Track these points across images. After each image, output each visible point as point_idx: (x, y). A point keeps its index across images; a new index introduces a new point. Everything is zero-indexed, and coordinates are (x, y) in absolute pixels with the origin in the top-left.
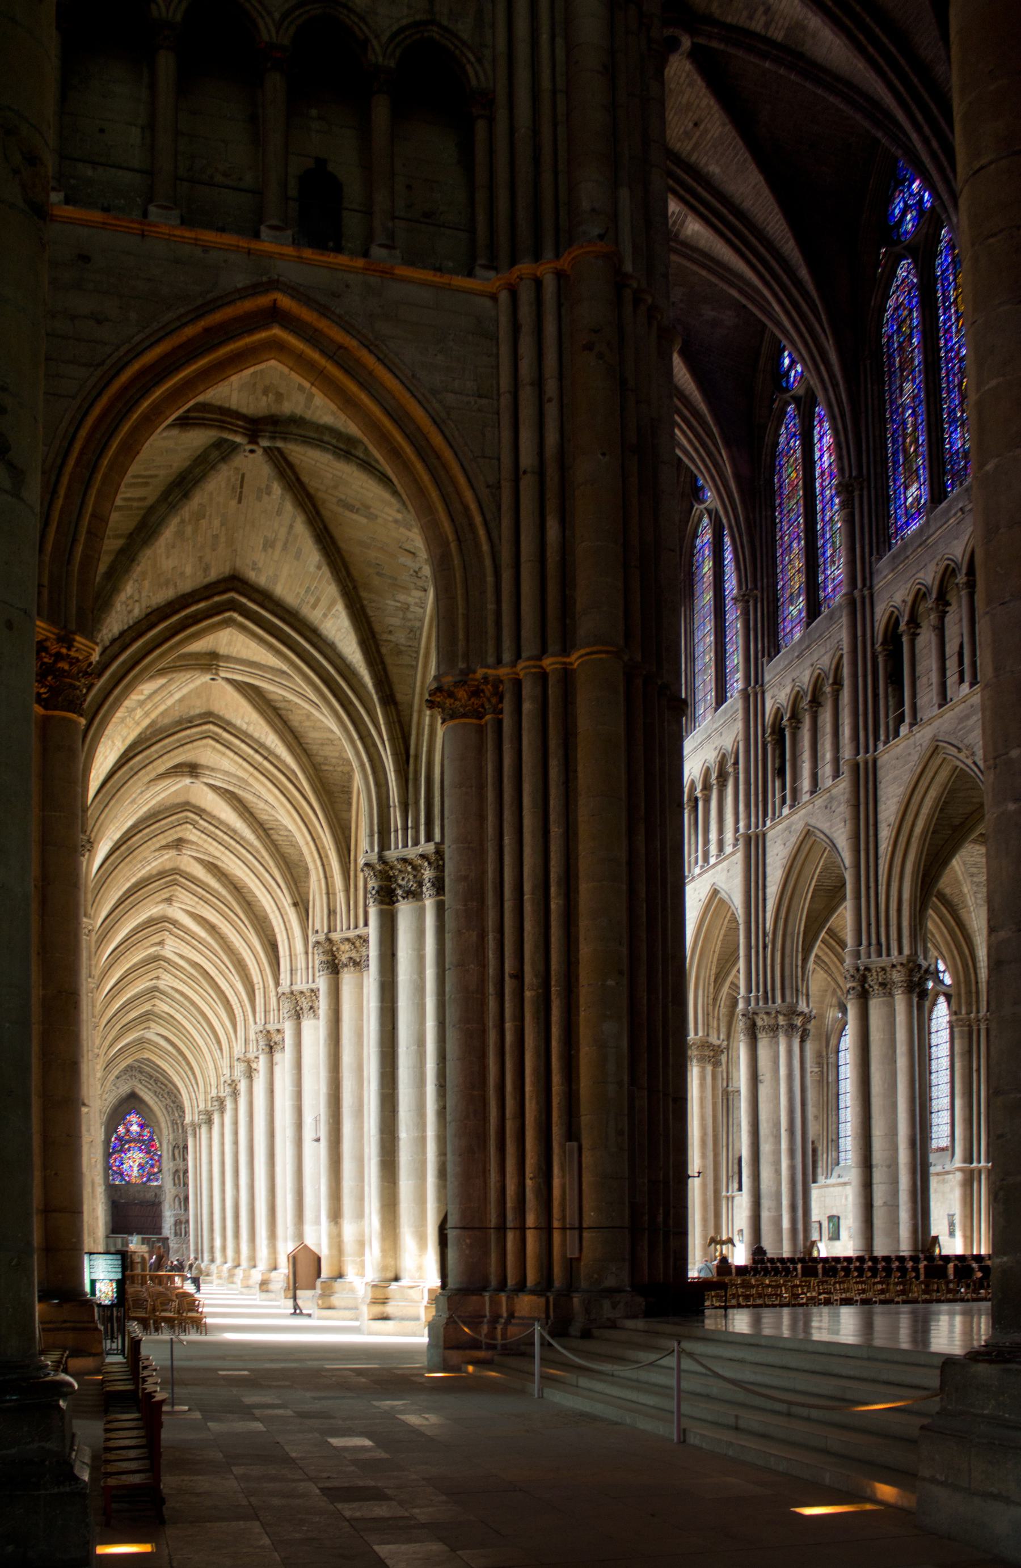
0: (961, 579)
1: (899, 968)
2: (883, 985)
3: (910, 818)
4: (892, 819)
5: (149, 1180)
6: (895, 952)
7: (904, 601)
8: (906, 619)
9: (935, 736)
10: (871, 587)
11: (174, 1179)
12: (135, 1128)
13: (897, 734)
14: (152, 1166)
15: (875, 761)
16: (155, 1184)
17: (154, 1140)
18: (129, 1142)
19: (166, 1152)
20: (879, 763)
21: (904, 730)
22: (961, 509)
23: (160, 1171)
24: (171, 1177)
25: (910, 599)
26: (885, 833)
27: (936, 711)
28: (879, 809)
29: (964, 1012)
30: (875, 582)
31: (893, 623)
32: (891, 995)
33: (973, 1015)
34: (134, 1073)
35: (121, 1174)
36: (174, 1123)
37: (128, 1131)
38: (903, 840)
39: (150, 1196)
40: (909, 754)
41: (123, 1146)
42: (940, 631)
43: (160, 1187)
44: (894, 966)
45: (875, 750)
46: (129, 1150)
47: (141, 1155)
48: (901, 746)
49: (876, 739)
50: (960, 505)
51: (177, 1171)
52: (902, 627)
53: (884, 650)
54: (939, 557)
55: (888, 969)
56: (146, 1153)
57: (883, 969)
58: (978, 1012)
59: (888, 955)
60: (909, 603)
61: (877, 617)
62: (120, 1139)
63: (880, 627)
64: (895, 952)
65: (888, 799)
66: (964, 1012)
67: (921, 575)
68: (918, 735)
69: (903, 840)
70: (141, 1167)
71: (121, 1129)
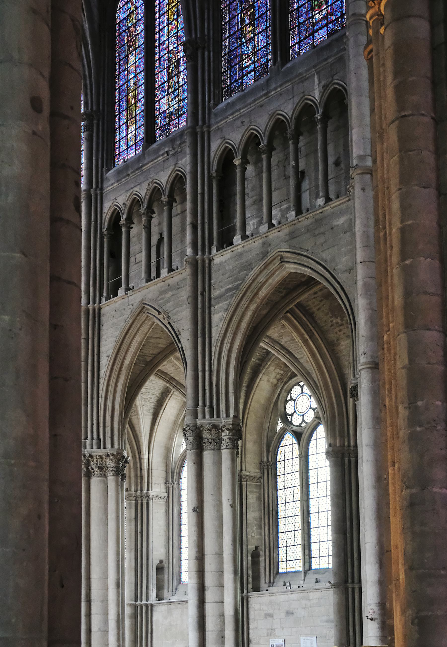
0: (165, 198)
1: (111, 457)
2: (101, 468)
3: (122, 353)
4: (110, 352)
6: (109, 445)
7: (124, 204)
8: (125, 216)
9: (143, 300)
10: (102, 189)
13: (116, 295)
15: (100, 309)
20: (103, 311)
21: (121, 291)
22: (167, 152)
25: (128, 204)
26: (105, 362)
27: (144, 284)
28: (101, 343)
29: (133, 489)
30: (105, 185)
31: (116, 216)
32: (105, 476)
33: (139, 492)
38: (116, 368)
40: (124, 309)
42: (148, 228)
44: (108, 456)
45: (100, 303)
48: (119, 303)
49: (101, 295)
50: (166, 150)
52: (123, 221)
53: (108, 234)
54: (150, 180)
55: (104, 457)
57: (101, 457)
58: (141, 490)
59: (105, 448)
60: (128, 206)
61: (105, 210)
63: (107, 216)
64: (109, 445)
65: (108, 338)
66: (133, 489)
67: (137, 189)
68: (131, 298)
69: (116, 368)
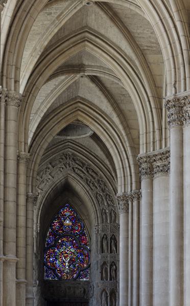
5: (79, 276)
11: (102, 273)
12: (68, 222)
14: (82, 262)
16: (85, 279)
17: (84, 235)
18: (61, 237)
19: (94, 246)
23: (89, 266)
24: (99, 270)
34: (68, 161)
35: (54, 271)
36: (103, 212)
37: (62, 224)
39: (79, 291)
41: (56, 241)
43: (88, 283)
46: (62, 245)
51: (105, 263)
56: (78, 248)
62: (54, 234)
70: (72, 261)
71: (56, 224)
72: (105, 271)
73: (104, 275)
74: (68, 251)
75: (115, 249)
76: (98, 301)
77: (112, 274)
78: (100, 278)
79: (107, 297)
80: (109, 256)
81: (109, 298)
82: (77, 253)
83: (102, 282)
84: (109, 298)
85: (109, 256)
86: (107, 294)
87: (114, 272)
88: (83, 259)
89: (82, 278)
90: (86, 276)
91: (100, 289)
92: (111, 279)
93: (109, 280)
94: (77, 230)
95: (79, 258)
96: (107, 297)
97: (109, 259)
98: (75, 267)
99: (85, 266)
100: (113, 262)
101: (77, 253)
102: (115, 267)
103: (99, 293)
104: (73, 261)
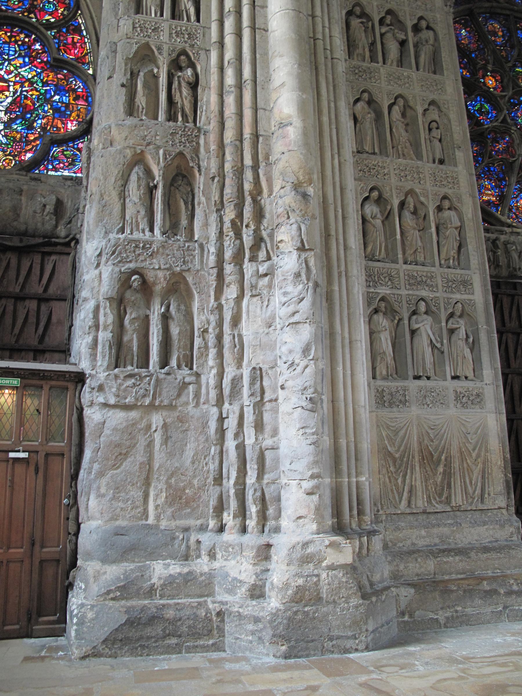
16: (66, 173)
24: (120, 77)
43: (78, 181)
47: (26, 73)
72: (145, 85)
73: (141, 100)
74: (9, 73)
75: (192, 11)
76: (104, 207)
77: (177, 98)
78: (121, 109)
79: (151, 190)
80: (165, 26)
81: (159, 194)
82: (45, 84)
83: (130, 121)
84: (159, 194)
85: (165, 26)
86: (148, 172)
87: (185, 91)
88: (67, 105)
89: (55, 169)
90: (72, 164)
91: (120, 152)
92: (171, 117)
93: (162, 116)
94: (51, 14)
95: (48, 101)
96: (151, 190)
97: (164, 37)
98: (30, 127)
99: (72, 127)
100: (184, 52)
101: (45, 84)
102: (189, 72)
103: (115, 172)
104: (26, 110)
